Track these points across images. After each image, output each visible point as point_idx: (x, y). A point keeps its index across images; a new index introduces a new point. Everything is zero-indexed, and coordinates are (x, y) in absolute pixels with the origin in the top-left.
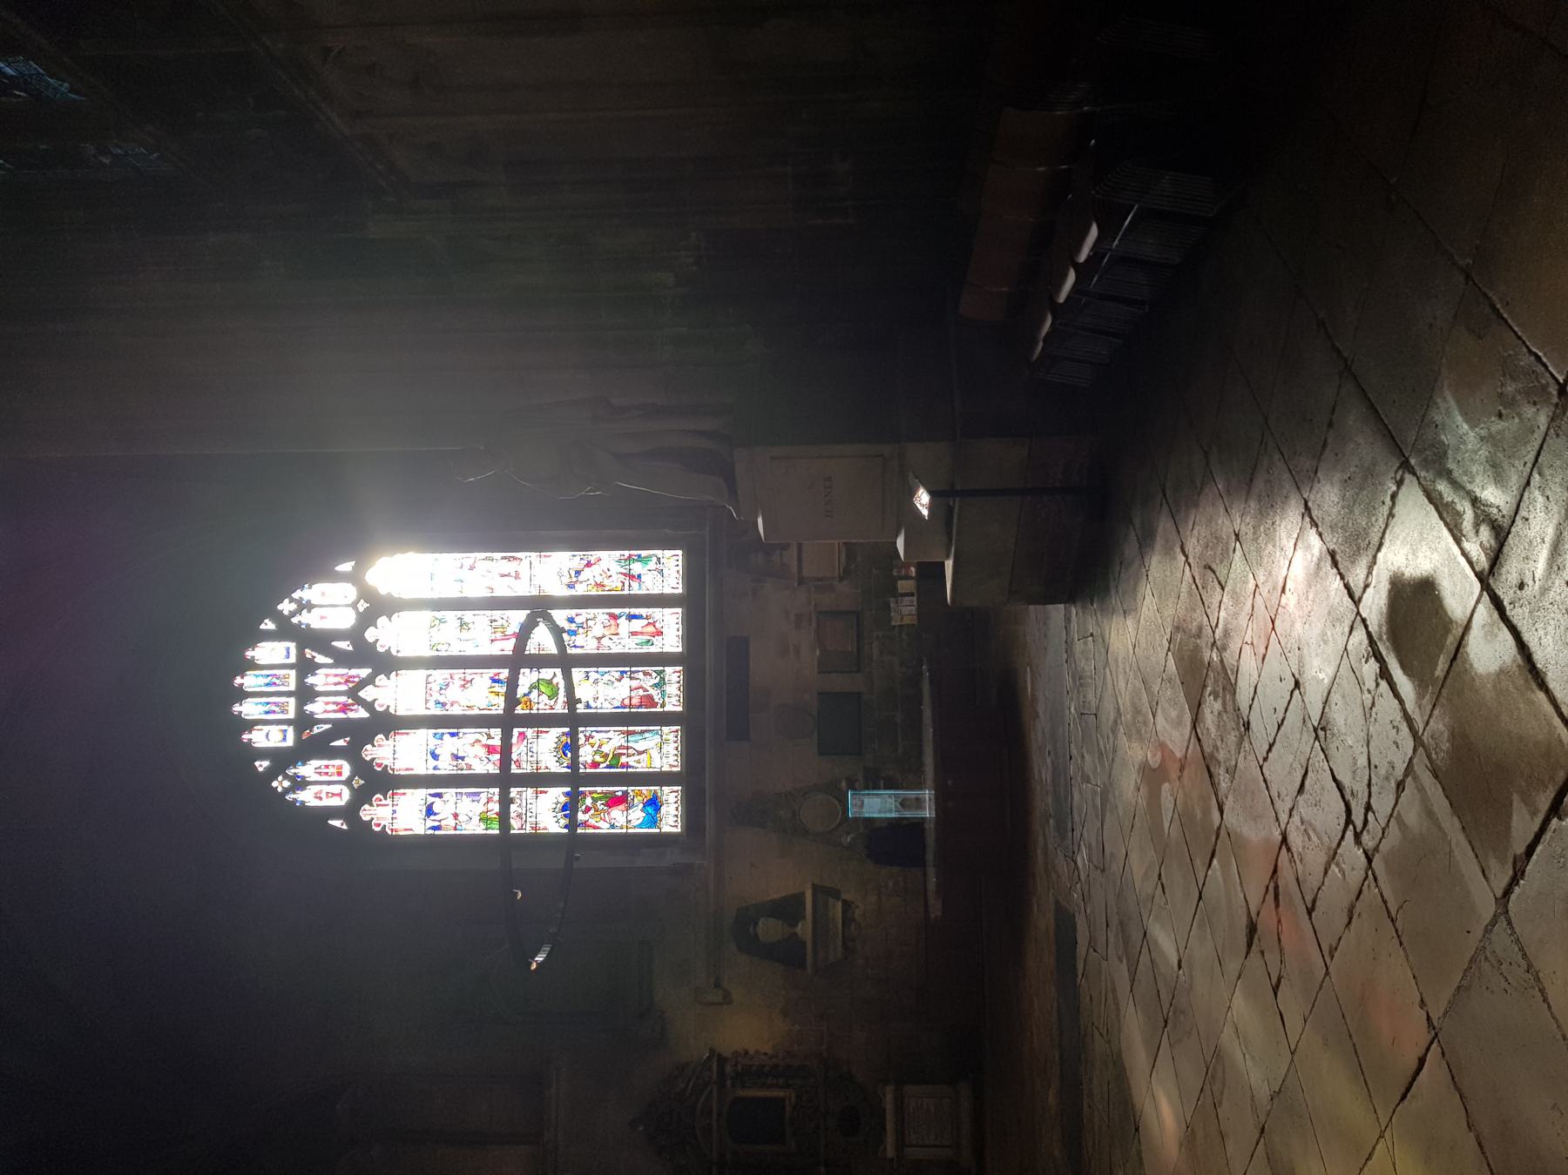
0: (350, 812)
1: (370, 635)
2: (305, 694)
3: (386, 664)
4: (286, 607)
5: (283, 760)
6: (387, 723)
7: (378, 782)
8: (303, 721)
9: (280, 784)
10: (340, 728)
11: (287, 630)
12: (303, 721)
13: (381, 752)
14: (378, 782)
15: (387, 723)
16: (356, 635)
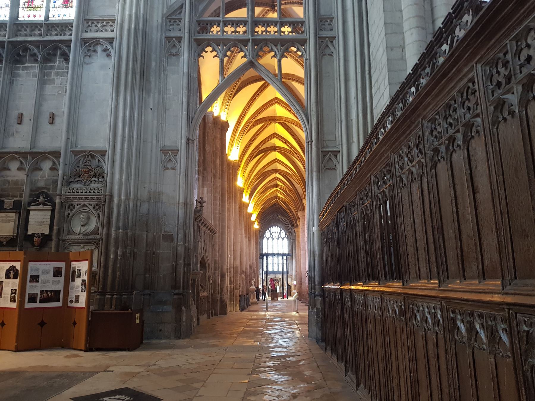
0: (265, 237)
1: (280, 238)
2: (275, 232)
3: (278, 239)
4: (283, 231)
5: (270, 231)
6: (273, 239)
7: (268, 239)
8: (273, 232)
9: (268, 230)
10: (272, 236)
11: (281, 231)
12: (273, 232)
13: (270, 239)
14: (268, 239)
15: (273, 239)
16: (280, 237)
